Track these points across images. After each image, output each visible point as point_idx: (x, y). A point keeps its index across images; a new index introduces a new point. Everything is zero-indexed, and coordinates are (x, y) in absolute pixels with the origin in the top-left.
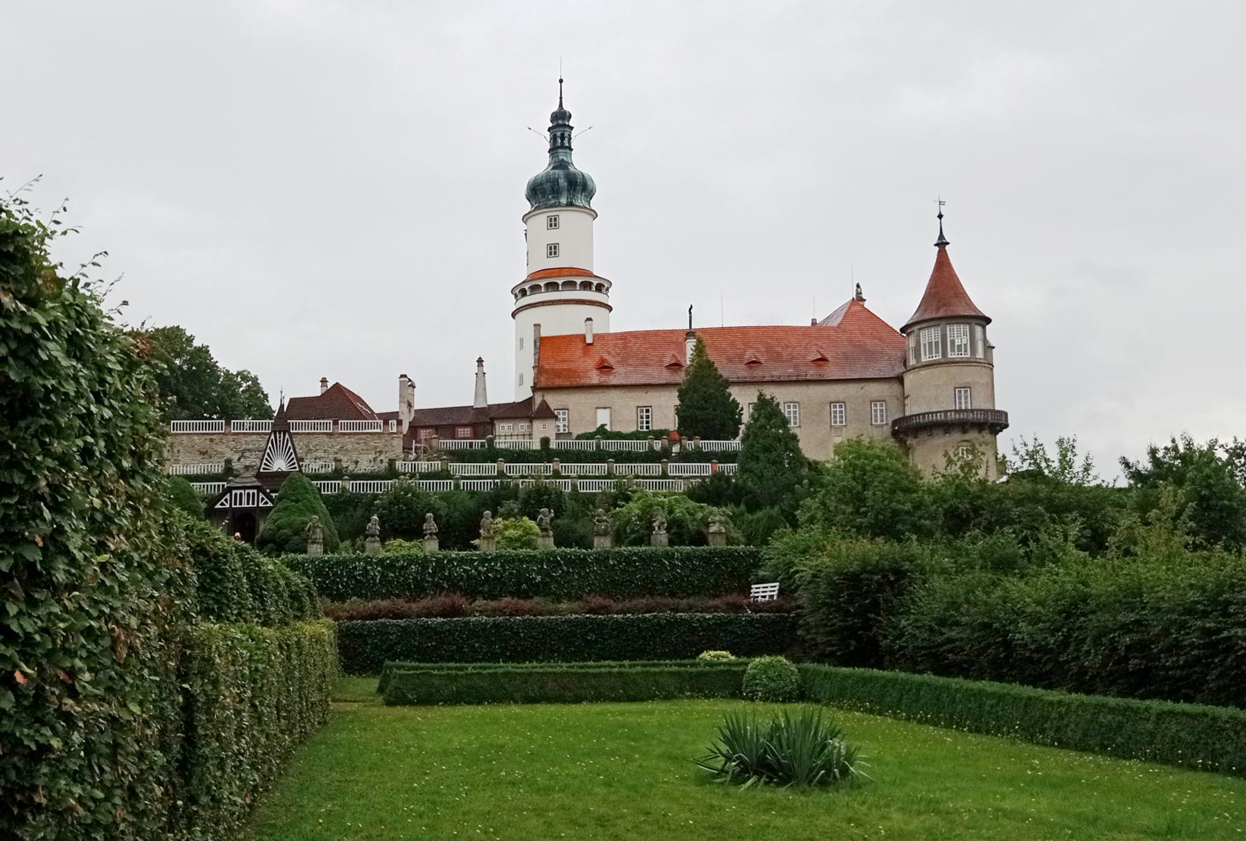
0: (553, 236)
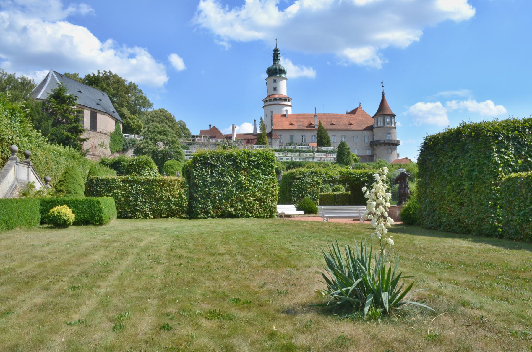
0: (275, 85)
